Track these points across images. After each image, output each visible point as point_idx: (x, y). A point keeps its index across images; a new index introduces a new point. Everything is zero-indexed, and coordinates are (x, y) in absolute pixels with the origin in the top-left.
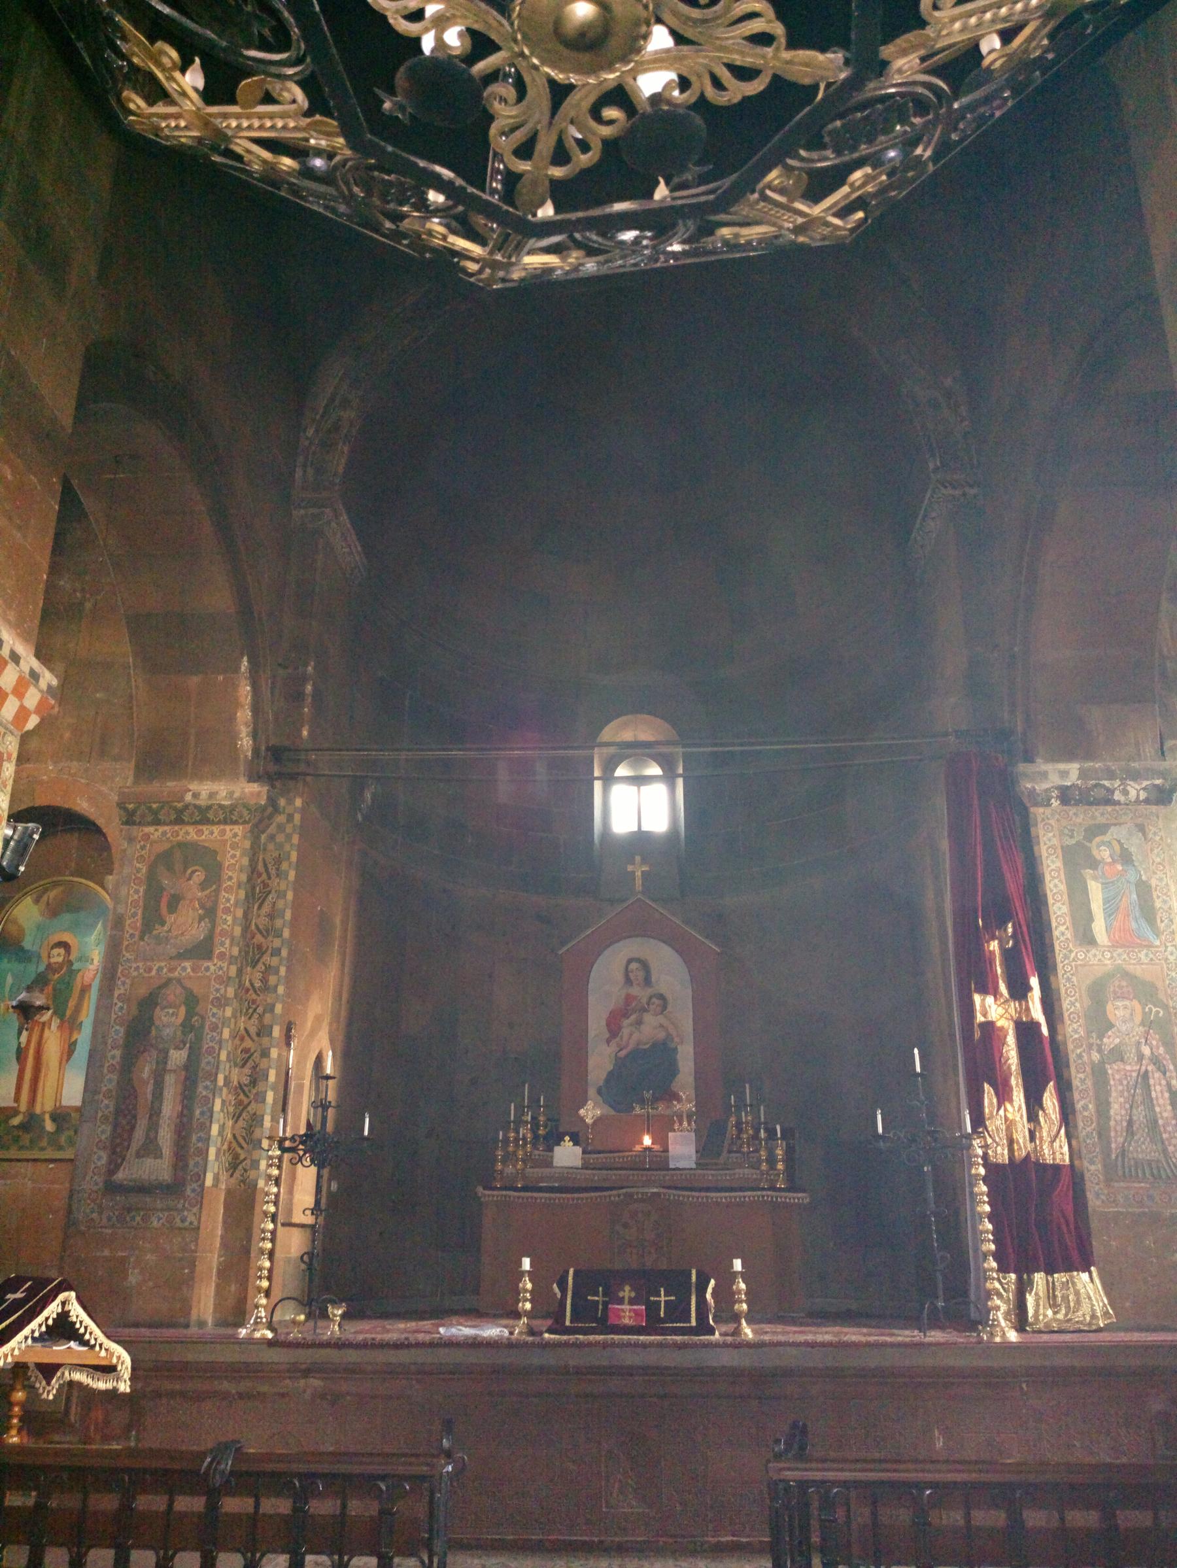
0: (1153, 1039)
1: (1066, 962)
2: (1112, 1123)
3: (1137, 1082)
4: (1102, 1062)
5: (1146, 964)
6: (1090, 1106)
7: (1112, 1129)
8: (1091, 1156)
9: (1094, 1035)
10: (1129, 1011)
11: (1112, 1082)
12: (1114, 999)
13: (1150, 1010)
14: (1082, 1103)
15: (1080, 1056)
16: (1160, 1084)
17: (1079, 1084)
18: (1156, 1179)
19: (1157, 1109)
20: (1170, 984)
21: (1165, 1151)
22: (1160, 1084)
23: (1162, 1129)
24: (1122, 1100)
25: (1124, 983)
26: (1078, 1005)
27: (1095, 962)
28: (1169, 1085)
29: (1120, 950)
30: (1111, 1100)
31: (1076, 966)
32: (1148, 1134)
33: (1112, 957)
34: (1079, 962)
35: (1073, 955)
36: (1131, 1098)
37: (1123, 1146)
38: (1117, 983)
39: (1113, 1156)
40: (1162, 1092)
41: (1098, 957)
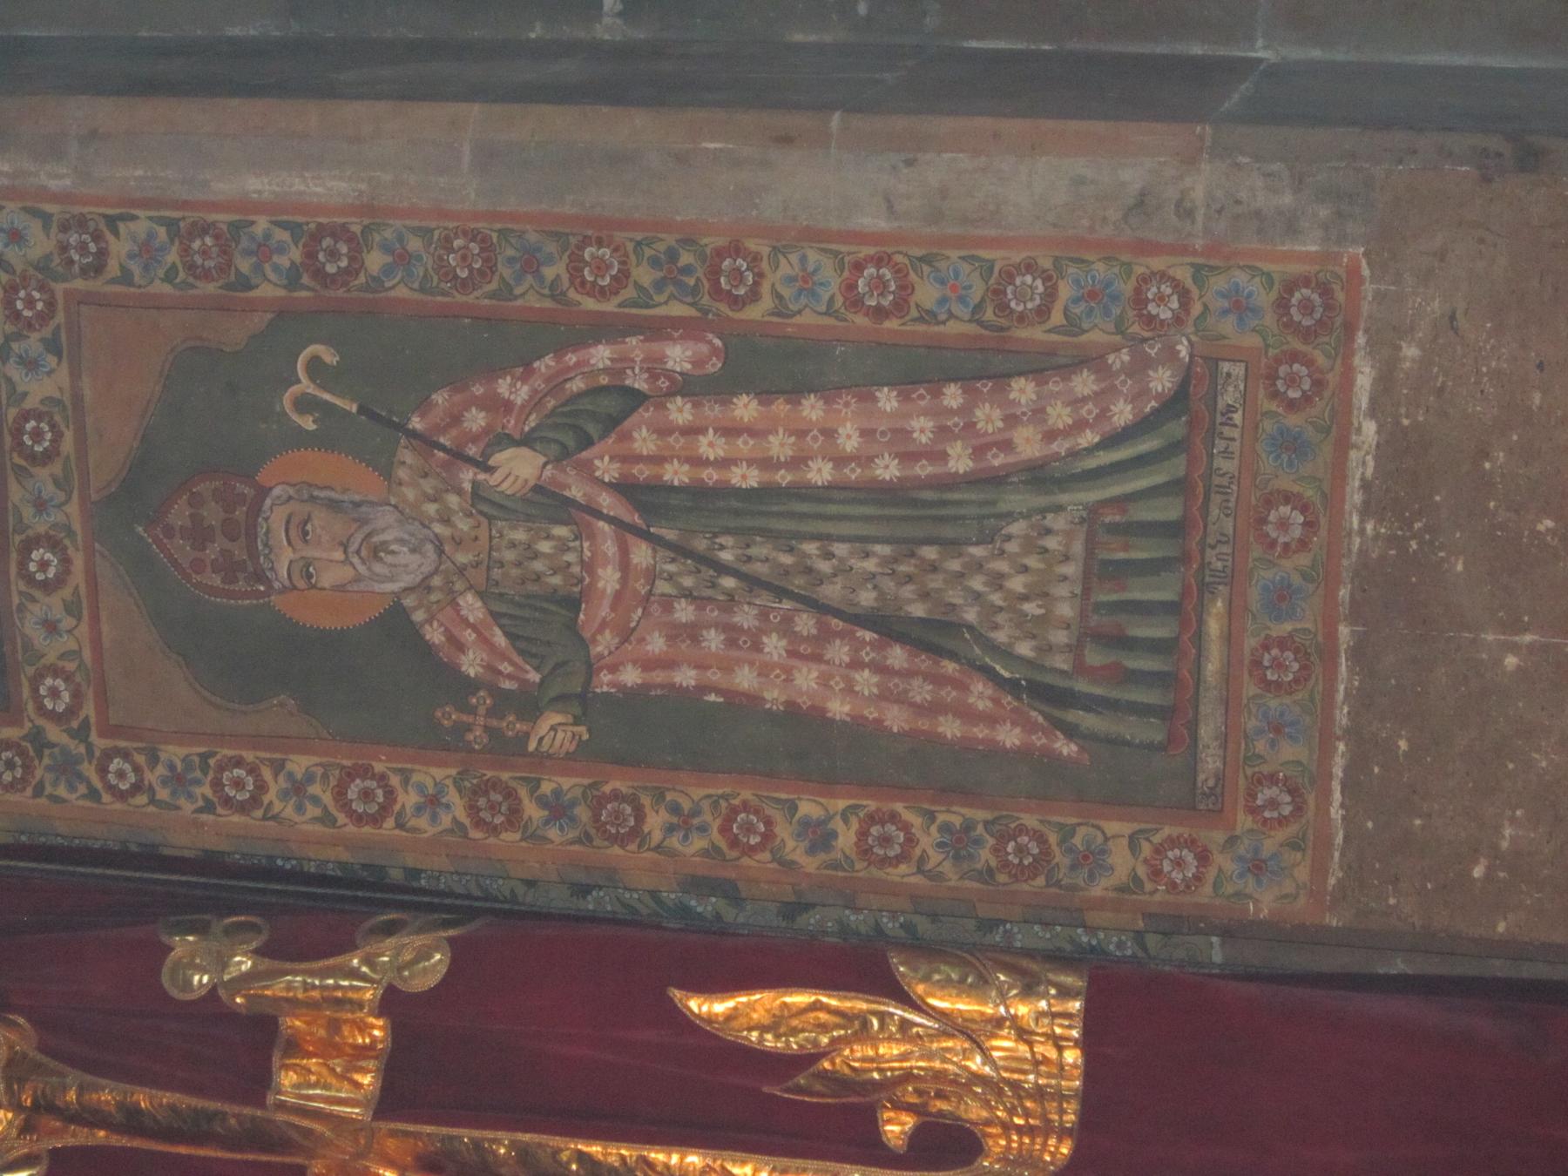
0: (456, 419)
1: (89, 770)
2: (896, 719)
3: (680, 551)
4: (584, 704)
5: (75, 375)
6: (808, 808)
7: (923, 724)
8: (1060, 858)
9: (449, 716)
10: (320, 520)
11: (686, 677)
12: (259, 576)
13: (305, 404)
14: (794, 849)
15: (558, 810)
16: (693, 431)
17: (698, 843)
18: (1185, 559)
19: (820, 473)
20: (170, 277)
21: (1039, 476)
22: (693, 431)
23: (923, 469)
24: (774, 646)
25: (179, 514)
26: (299, 764)
27: (84, 628)
28: (687, 387)
29: (16, 493)
30: (774, 696)
31: (109, 731)
32: (951, 546)
33: (54, 545)
34: (89, 710)
35: (54, 733)
36: (765, 599)
37: (1012, 686)
38: (182, 549)
39: (1066, 748)
40: (730, 431)
41: (58, 612)
